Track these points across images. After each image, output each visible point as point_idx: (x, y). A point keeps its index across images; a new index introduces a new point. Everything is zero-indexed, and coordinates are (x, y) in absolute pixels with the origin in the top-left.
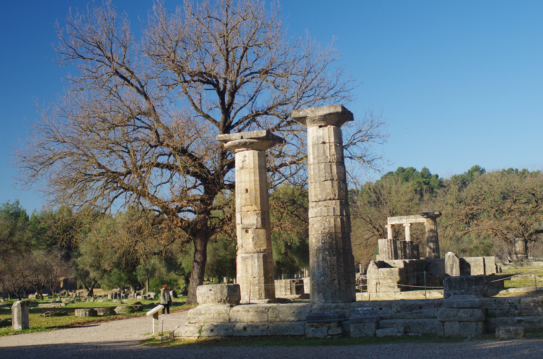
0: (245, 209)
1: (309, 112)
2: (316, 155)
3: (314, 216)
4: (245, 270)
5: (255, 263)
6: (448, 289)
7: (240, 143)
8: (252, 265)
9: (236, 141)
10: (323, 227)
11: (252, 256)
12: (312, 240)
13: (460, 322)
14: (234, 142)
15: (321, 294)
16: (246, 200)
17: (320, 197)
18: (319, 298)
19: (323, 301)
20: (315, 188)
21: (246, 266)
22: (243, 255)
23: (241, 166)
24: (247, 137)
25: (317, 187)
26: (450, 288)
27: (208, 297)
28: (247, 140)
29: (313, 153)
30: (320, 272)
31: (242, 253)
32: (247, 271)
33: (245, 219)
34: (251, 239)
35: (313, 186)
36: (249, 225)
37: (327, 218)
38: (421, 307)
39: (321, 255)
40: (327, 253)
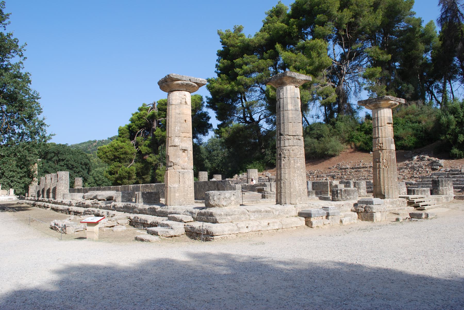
0: (183, 135)
5: (190, 177)
7: (187, 84)
9: (185, 82)
10: (300, 153)
14: (182, 82)
17: (297, 133)
21: (185, 178)
22: (180, 170)
23: (180, 101)
24: (194, 81)
25: (295, 126)
28: (194, 84)
33: (183, 143)
36: (186, 148)
40: (302, 170)
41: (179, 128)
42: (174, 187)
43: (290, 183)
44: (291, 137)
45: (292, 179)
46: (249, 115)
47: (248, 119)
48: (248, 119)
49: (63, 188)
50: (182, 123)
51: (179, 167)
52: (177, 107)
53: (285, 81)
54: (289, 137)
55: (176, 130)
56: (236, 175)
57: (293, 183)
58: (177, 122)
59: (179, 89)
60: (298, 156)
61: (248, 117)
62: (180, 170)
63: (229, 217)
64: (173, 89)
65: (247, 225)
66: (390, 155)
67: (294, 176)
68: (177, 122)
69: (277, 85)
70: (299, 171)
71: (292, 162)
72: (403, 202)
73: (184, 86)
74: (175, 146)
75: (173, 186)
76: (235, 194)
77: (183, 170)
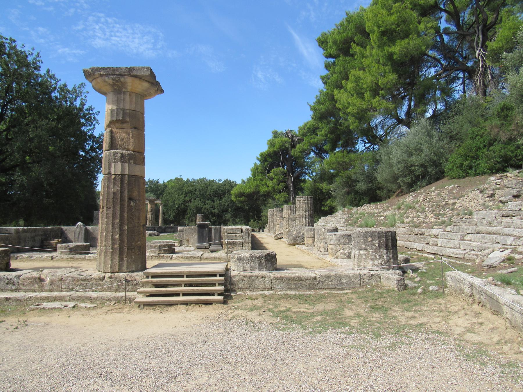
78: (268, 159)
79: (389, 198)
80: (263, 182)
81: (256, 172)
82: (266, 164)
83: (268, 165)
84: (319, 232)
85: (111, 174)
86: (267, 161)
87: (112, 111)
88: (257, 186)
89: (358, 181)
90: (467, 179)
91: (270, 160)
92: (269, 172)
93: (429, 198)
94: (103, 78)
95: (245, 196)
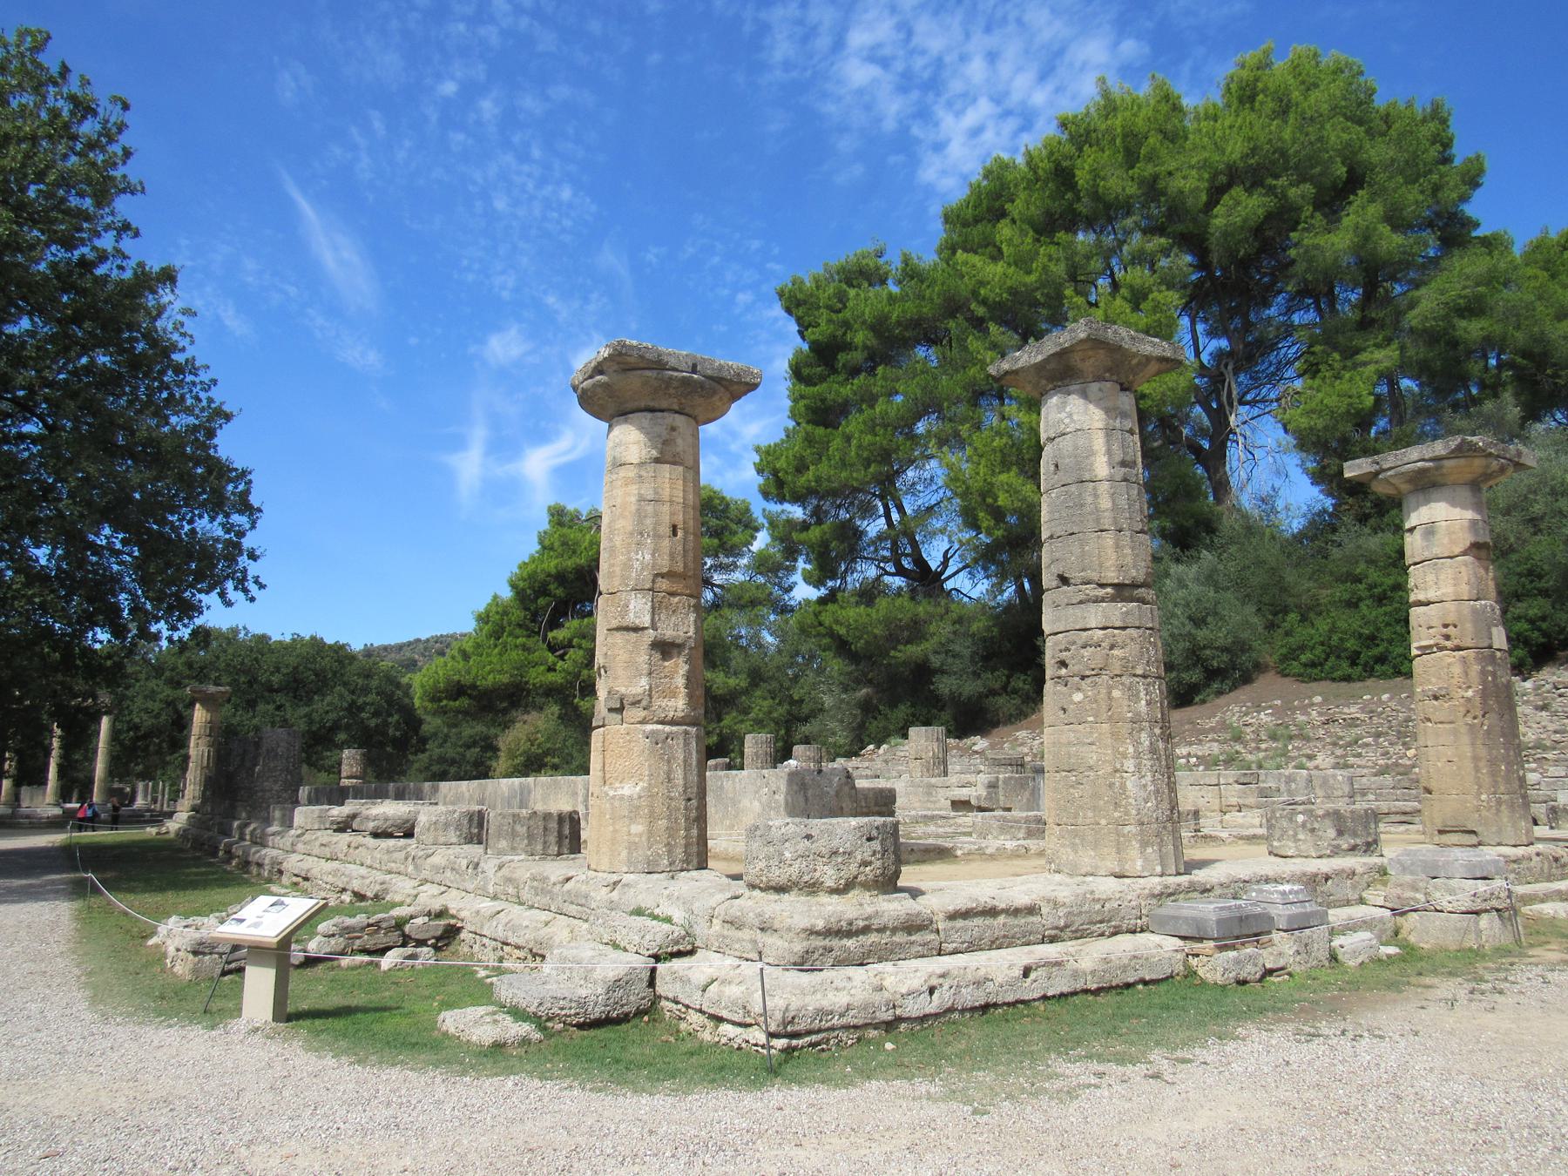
1: (1127, 339)
2: (1119, 457)
3: (1118, 624)
4: (663, 776)
6: (1332, 833)
8: (685, 761)
9: (676, 374)
11: (686, 733)
12: (1110, 693)
13: (1498, 910)
15: (1149, 850)
16: (672, 556)
18: (1146, 860)
19: (1159, 869)
20: (1117, 546)
21: (669, 762)
25: (1124, 546)
26: (1340, 833)
27: (865, 864)
29: (1109, 452)
30: (1145, 786)
31: (643, 722)
32: (670, 780)
33: (663, 617)
34: (680, 681)
35: (1110, 542)
37: (1151, 635)
38: (1327, 878)
39: (1144, 735)
41: (648, 557)
42: (622, 798)
43: (1111, 785)
44: (1109, 590)
45: (1118, 766)
46: (909, 550)
47: (907, 563)
48: (907, 563)
49: (276, 787)
50: (660, 537)
51: (642, 714)
52: (643, 473)
53: (1080, 365)
54: (1101, 592)
55: (637, 565)
56: (871, 747)
57: (1123, 786)
58: (641, 534)
59: (652, 404)
60: (1139, 672)
61: (907, 555)
62: (649, 727)
63: (850, 943)
64: (630, 406)
65: (934, 981)
66: (1490, 668)
67: (1124, 756)
68: (641, 534)
69: (1044, 382)
70: (1144, 735)
71: (1116, 693)
72: (1556, 860)
73: (672, 391)
74: (636, 629)
75: (620, 792)
76: (874, 833)
77: (660, 727)
78: (552, 587)
79: (1026, 716)
80: (536, 656)
81: (495, 623)
82: (542, 601)
83: (548, 605)
84: (1332, 781)
85: (1490, 647)
86: (549, 595)
87: (1473, 523)
88: (521, 667)
89: (943, 672)
90: (1370, 682)
91: (560, 592)
92: (554, 624)
93: (1344, 720)
94: (1490, 460)
95: (470, 696)
